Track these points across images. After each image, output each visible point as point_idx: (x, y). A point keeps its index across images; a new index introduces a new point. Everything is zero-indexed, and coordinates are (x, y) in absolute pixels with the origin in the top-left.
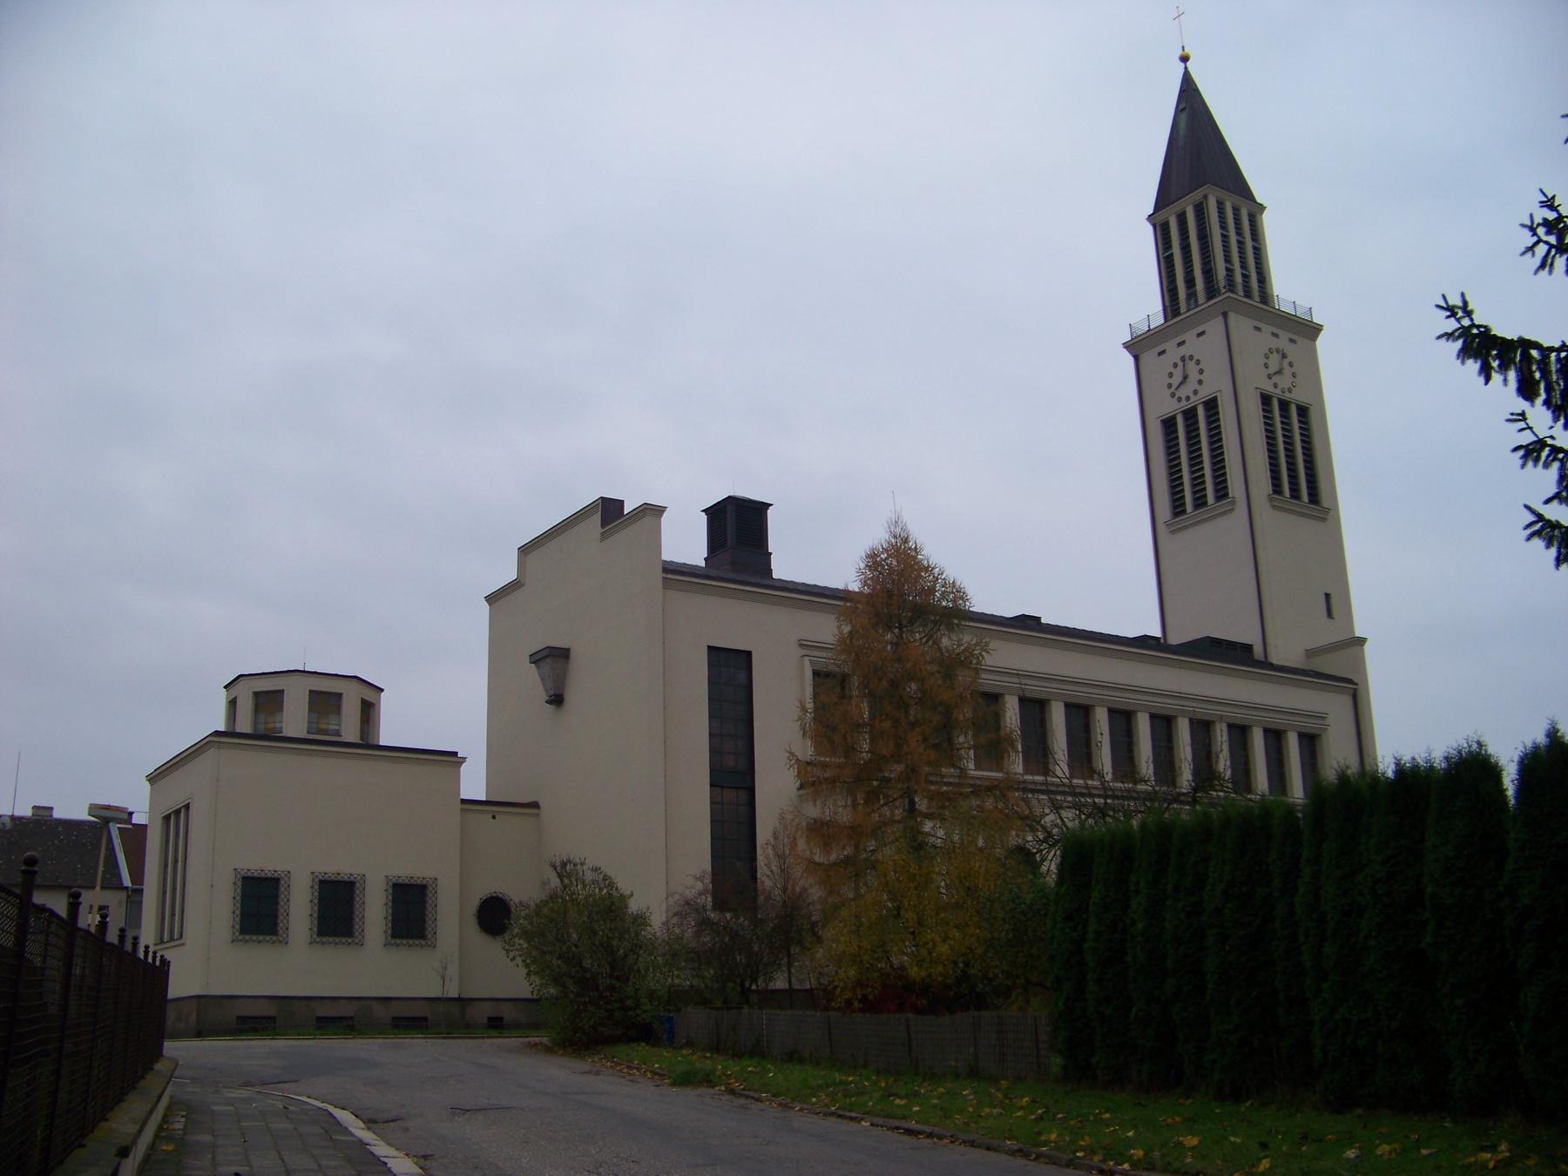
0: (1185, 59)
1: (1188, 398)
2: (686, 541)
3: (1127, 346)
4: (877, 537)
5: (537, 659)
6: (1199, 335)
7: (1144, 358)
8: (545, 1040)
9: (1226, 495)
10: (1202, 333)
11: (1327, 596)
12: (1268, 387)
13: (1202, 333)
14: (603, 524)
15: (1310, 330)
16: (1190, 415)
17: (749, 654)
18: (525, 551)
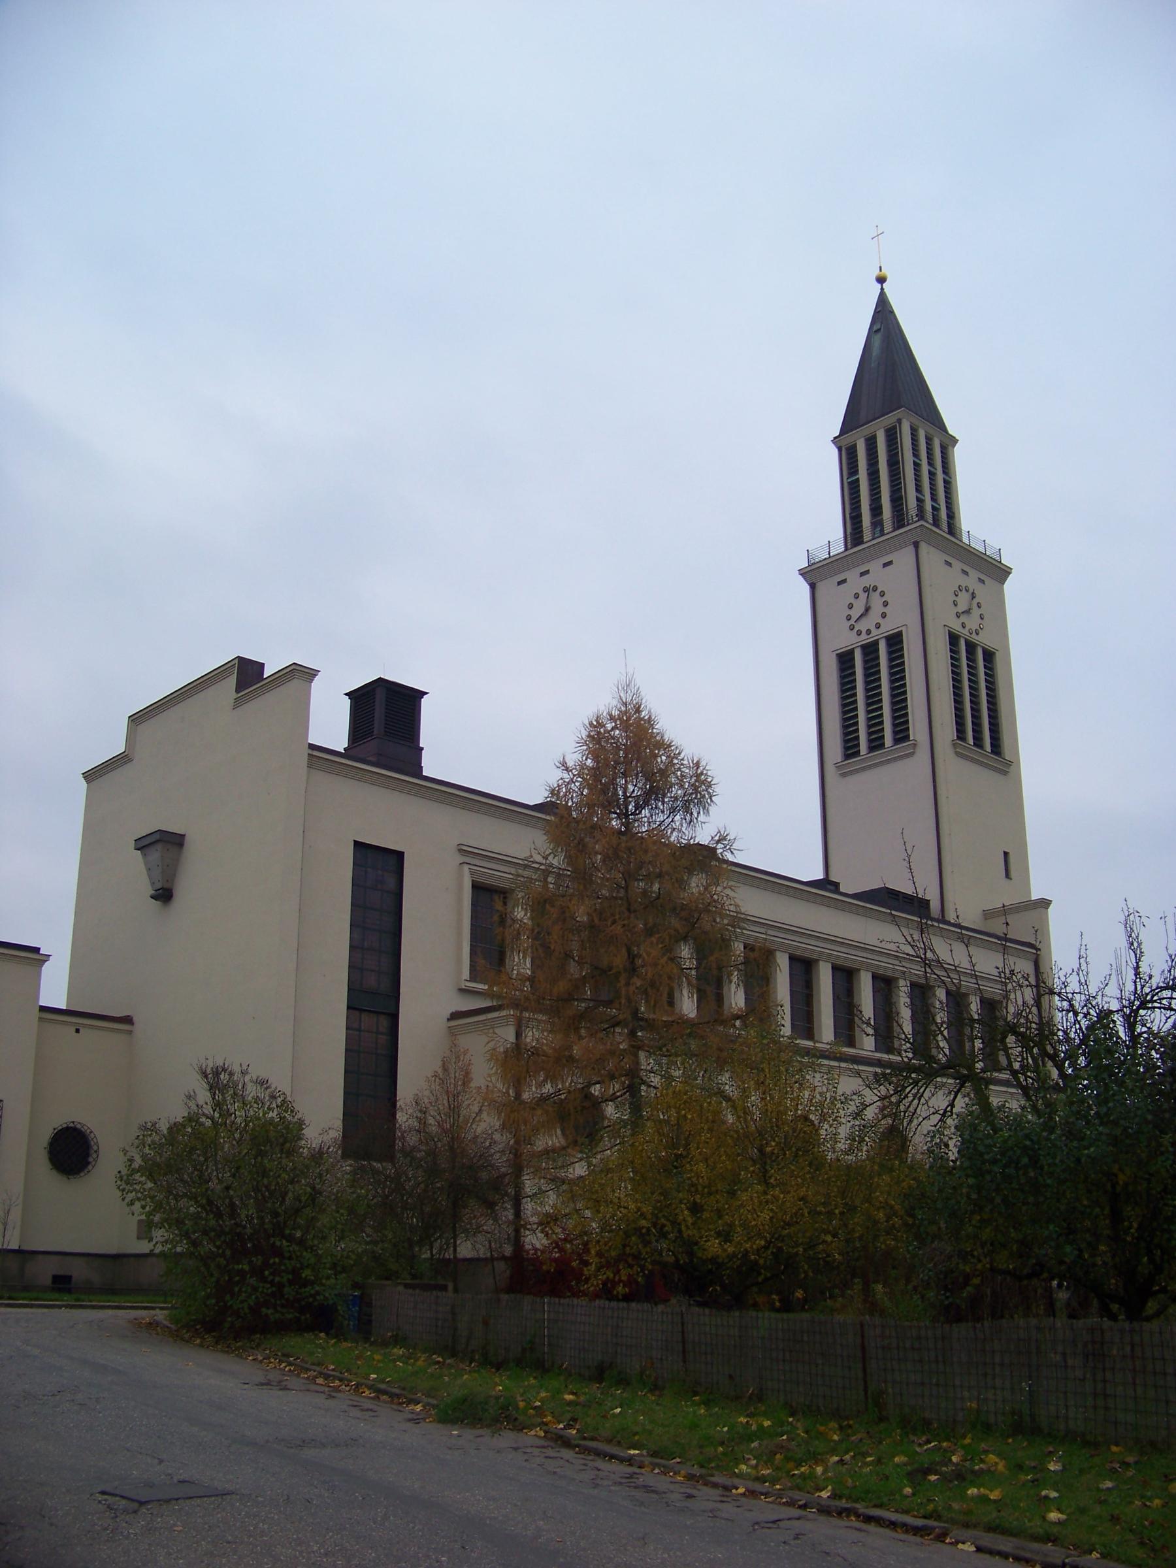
0: (881, 280)
1: (869, 632)
2: (330, 725)
3: (803, 573)
4: (602, 701)
5: (144, 845)
6: (885, 565)
7: (820, 587)
8: (160, 1315)
9: (907, 738)
10: (890, 563)
11: (1006, 854)
12: (956, 626)
13: (890, 563)
14: (237, 691)
15: (1000, 573)
16: (870, 650)
17: (400, 855)
18: (137, 719)
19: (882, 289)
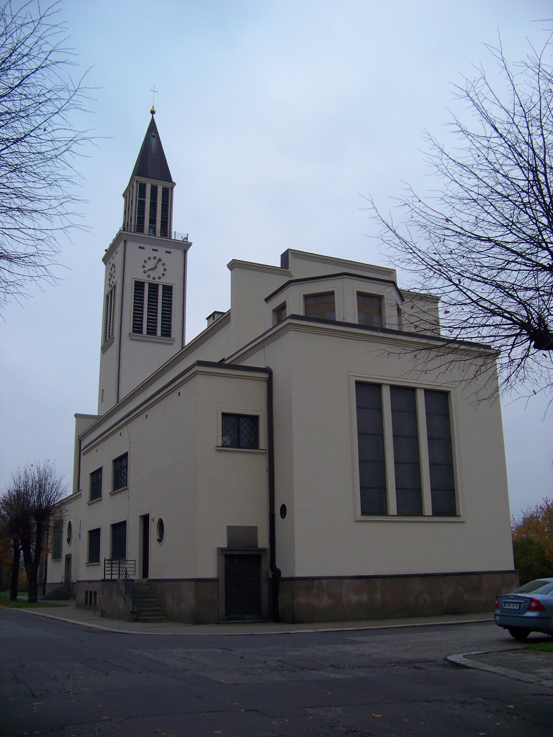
0: (153, 112)
1: (154, 278)
9: (169, 335)
19: (153, 117)
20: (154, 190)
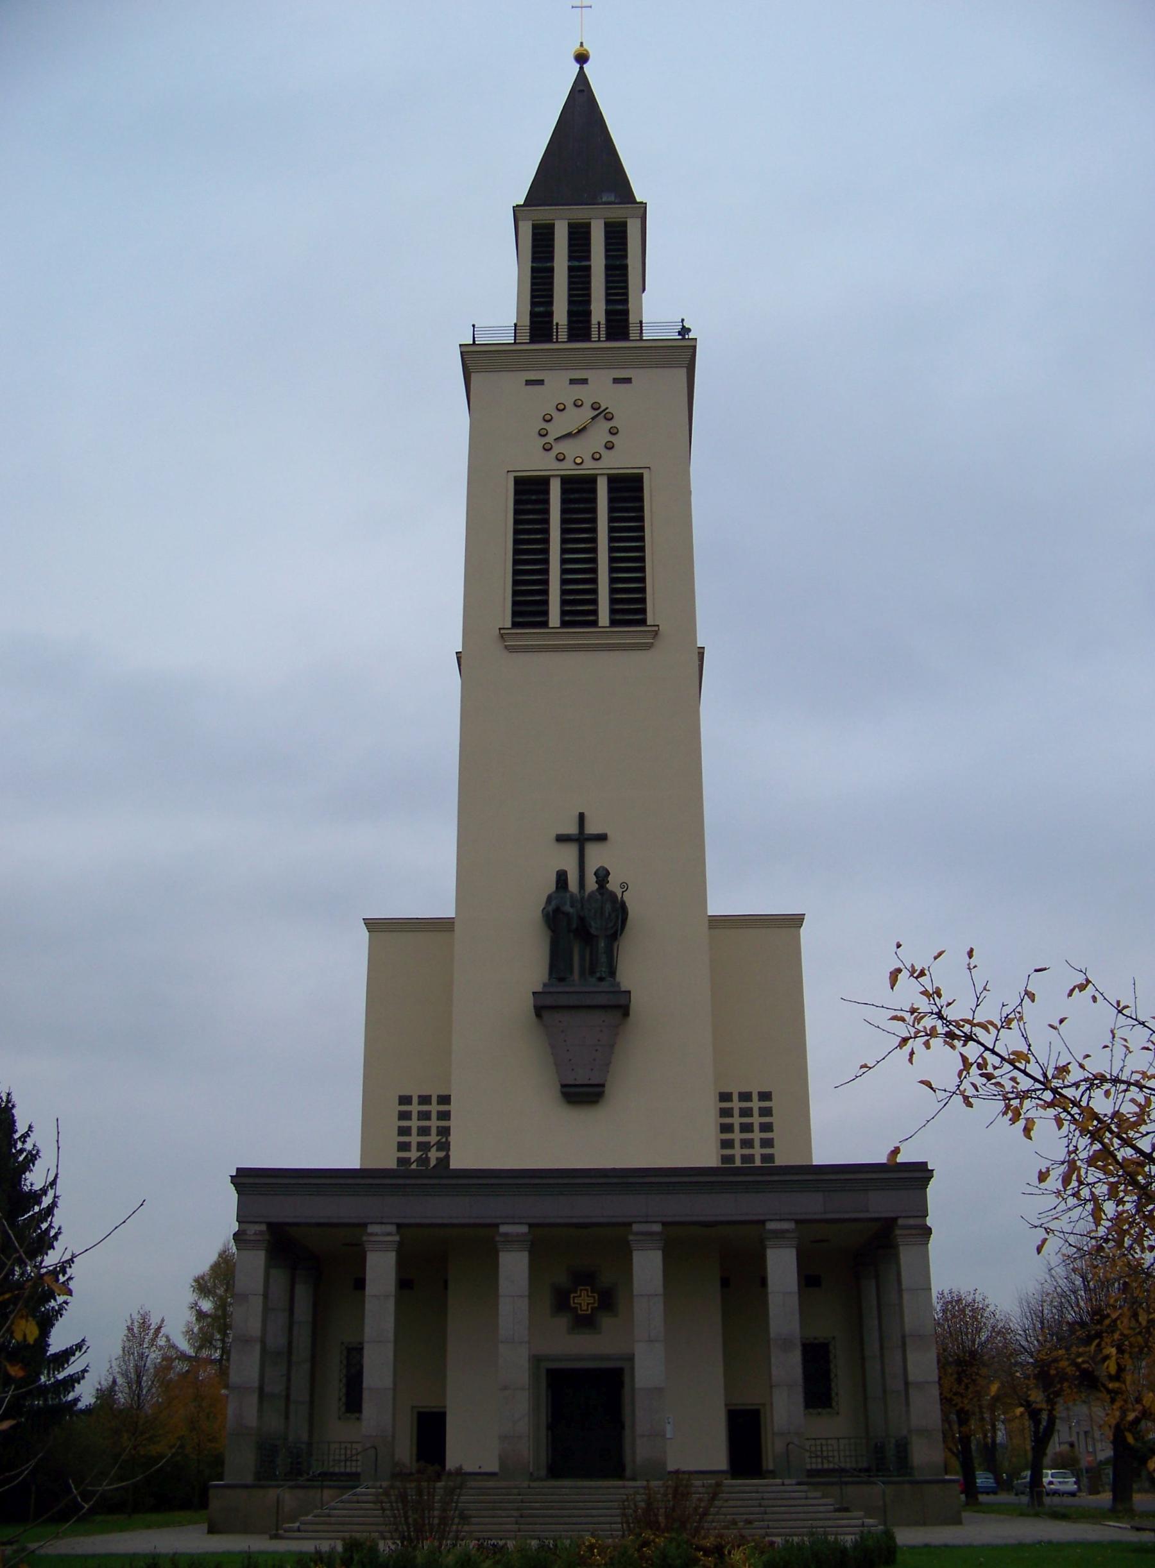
0: (582, 58)
19: (581, 68)
20: (579, 237)
